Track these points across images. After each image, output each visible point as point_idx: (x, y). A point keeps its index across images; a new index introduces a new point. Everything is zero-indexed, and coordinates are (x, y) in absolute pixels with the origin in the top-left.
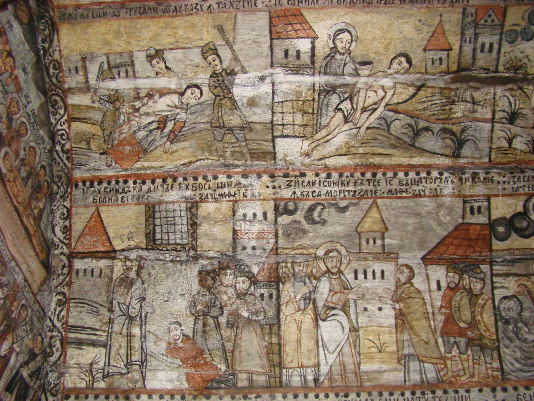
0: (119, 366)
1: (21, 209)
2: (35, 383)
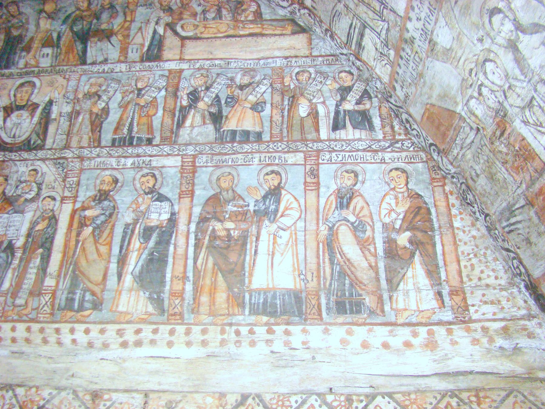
0: (381, 27)
1: (231, 32)
2: (372, 103)
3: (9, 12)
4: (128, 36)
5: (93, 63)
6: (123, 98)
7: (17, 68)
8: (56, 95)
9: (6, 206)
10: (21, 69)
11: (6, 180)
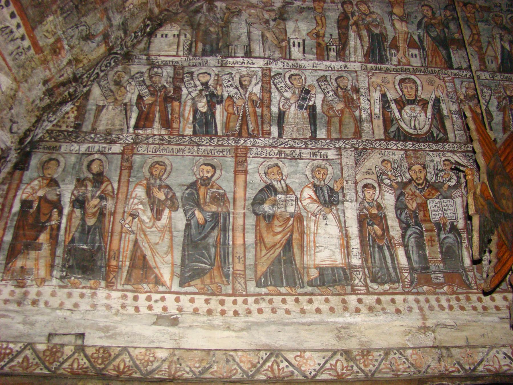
3: (360, 10)
4: (481, 48)
5: (460, 69)
6: (499, 103)
7: (391, 64)
8: (439, 94)
9: (433, 192)
10: (396, 66)
11: (424, 168)
